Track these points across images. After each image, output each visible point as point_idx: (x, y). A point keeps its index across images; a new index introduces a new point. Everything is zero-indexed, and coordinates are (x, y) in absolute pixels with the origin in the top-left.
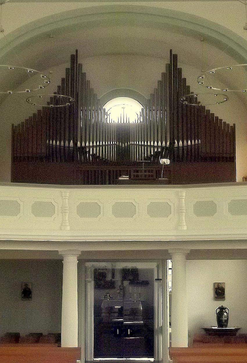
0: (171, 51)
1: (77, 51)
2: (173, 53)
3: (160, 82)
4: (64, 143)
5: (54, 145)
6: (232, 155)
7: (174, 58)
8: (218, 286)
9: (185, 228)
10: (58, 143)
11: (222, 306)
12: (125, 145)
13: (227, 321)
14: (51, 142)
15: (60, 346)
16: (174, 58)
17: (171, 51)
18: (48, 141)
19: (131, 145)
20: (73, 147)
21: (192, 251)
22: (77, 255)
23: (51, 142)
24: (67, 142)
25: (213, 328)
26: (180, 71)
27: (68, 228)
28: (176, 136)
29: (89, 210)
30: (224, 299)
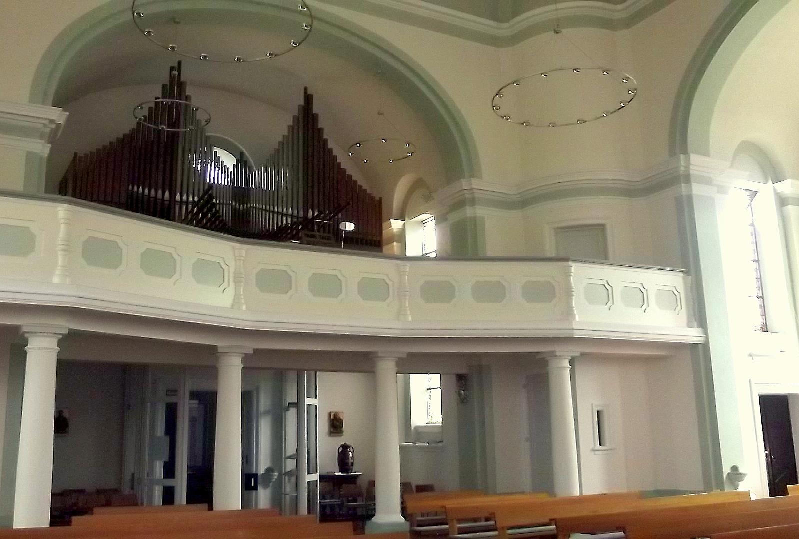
0: (306, 89)
1: (180, 63)
2: (309, 93)
3: (291, 128)
4: (156, 192)
5: (140, 193)
6: (378, 238)
7: (308, 99)
8: (335, 416)
9: (410, 319)
10: (147, 190)
11: (345, 443)
12: (243, 207)
13: (352, 464)
14: (136, 188)
15: (211, 508)
16: (308, 99)
17: (306, 89)
18: (130, 187)
19: (251, 209)
20: (170, 201)
21: (411, 355)
22: (242, 354)
23: (136, 188)
24: (160, 192)
25: (337, 474)
26: (315, 118)
27: (244, 307)
28: (310, 203)
29: (276, 282)
30: (341, 434)
